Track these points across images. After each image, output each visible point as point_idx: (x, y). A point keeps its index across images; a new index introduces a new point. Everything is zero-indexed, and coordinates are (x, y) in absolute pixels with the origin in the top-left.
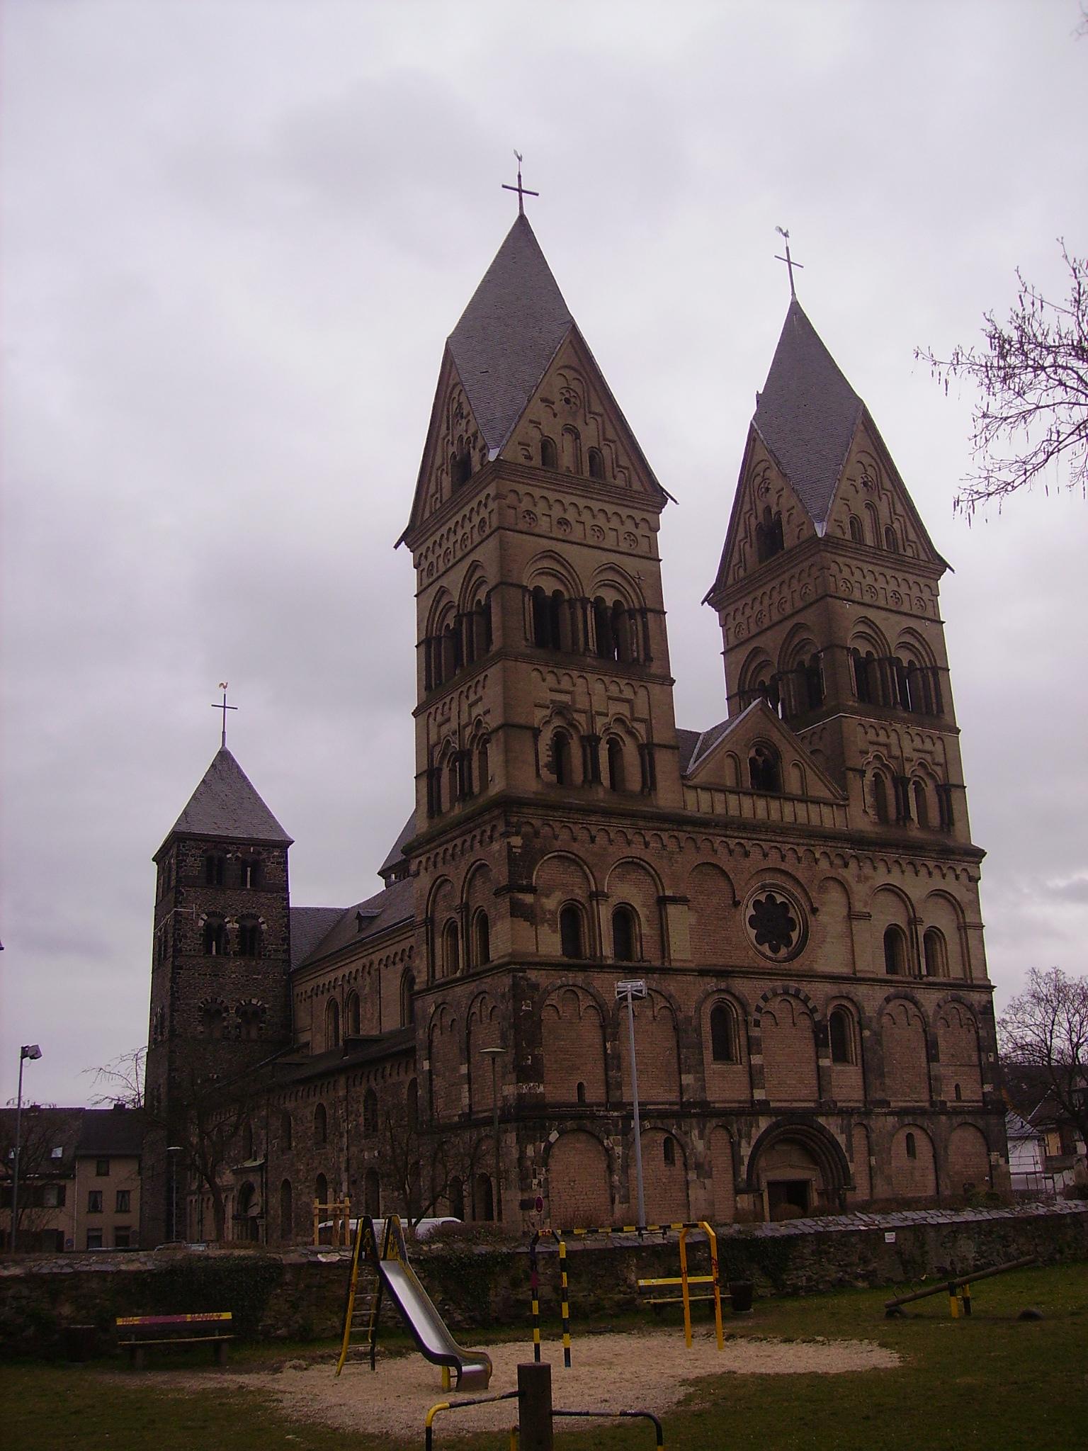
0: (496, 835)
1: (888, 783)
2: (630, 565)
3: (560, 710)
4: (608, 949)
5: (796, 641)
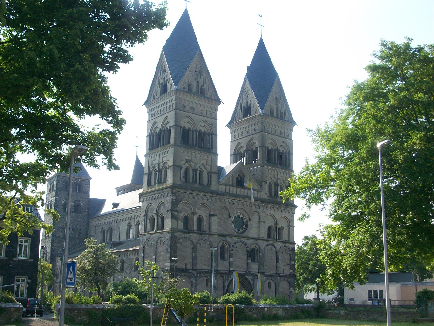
0: (168, 195)
1: (273, 186)
2: (210, 120)
3: (188, 161)
4: (195, 228)
5: (252, 142)
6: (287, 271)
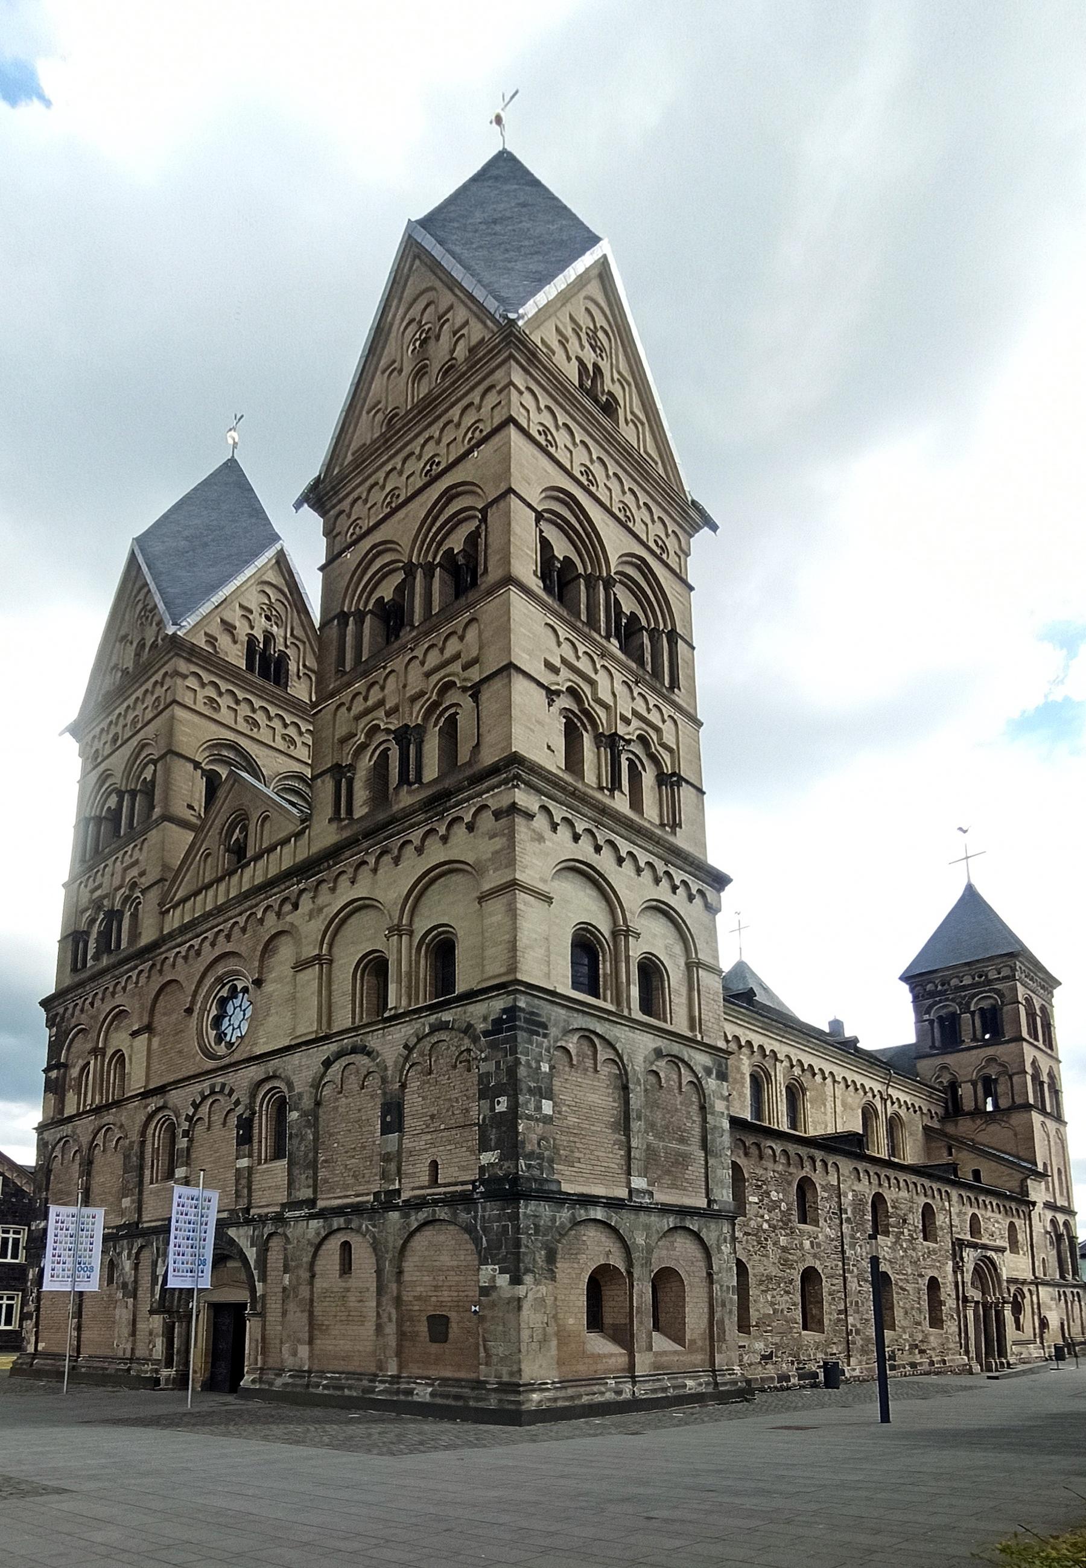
6: (462, 1164)
